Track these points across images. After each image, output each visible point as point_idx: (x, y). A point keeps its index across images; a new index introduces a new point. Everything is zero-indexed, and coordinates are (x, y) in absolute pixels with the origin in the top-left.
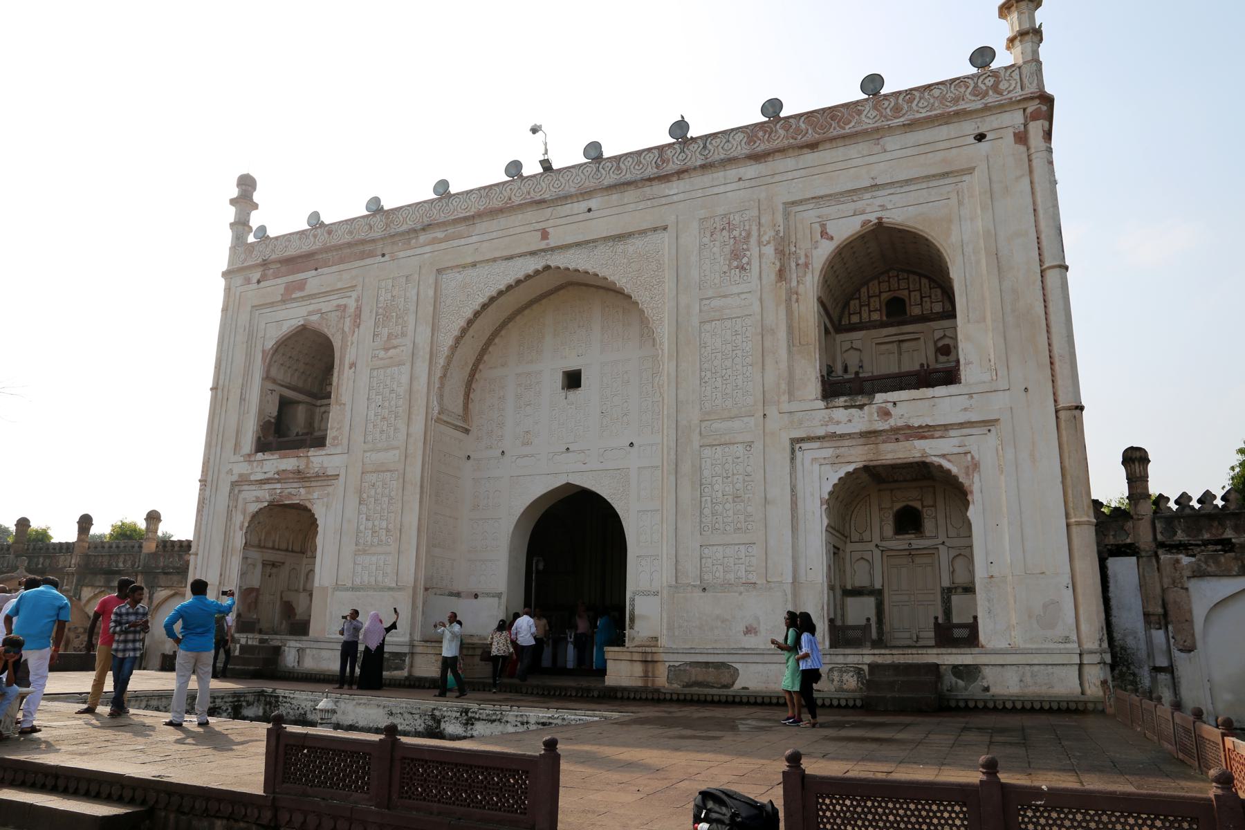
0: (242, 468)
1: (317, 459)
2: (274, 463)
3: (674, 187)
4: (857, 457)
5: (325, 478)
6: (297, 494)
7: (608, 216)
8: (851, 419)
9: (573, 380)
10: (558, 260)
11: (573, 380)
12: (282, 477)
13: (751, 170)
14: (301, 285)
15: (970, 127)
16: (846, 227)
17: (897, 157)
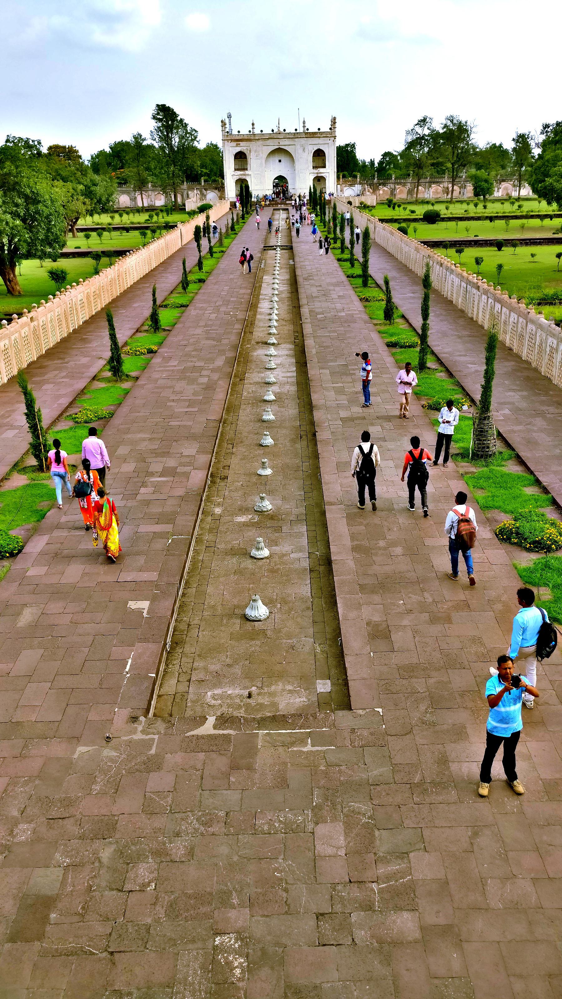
0: (234, 173)
1: (247, 172)
2: (239, 173)
3: (296, 139)
4: (316, 175)
5: (248, 175)
6: (244, 177)
7: (287, 142)
8: (316, 171)
9: (280, 161)
10: (281, 147)
11: (280, 161)
12: (241, 175)
13: (305, 139)
14: (239, 144)
15: (329, 138)
16: (316, 149)
17: (321, 141)
